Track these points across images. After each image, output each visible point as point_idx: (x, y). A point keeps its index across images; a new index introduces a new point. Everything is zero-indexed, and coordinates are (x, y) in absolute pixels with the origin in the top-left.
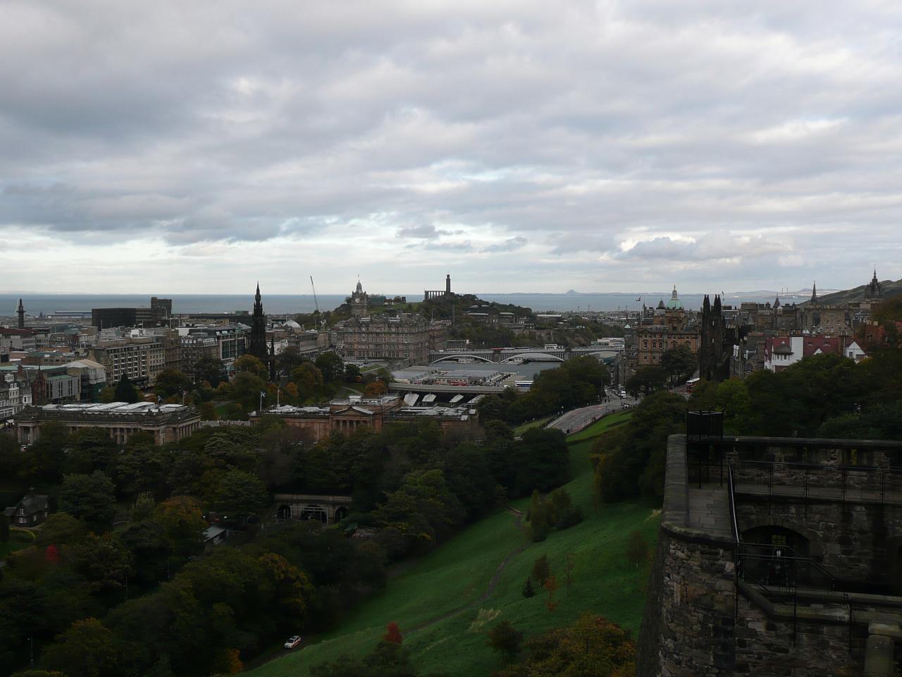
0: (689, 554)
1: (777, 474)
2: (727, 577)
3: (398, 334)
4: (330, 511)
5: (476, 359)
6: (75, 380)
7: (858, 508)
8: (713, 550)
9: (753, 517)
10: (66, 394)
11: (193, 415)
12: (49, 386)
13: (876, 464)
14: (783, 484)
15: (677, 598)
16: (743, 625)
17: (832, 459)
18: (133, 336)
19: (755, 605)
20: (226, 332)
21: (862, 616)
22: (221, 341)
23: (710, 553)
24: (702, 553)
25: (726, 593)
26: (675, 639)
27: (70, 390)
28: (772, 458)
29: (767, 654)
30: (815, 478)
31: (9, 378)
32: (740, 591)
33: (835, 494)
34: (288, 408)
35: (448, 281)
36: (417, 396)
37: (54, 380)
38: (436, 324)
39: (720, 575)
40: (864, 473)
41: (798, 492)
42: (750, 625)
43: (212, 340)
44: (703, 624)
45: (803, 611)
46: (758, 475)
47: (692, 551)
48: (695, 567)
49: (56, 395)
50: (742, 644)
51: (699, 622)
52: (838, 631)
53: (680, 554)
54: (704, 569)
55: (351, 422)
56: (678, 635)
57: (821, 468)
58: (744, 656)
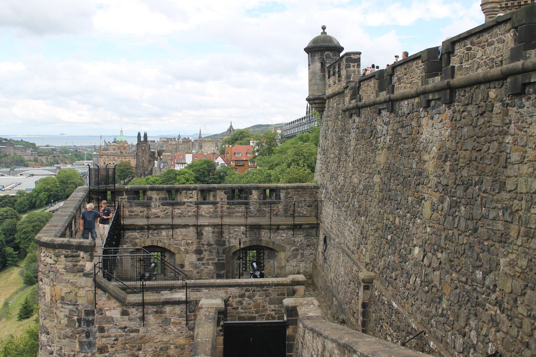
0: (56, 259)
1: (154, 211)
2: (86, 275)
7: (207, 229)
8: (74, 254)
9: (137, 241)
13: (218, 200)
14: (158, 217)
15: (48, 298)
16: (102, 314)
17: (190, 198)
19: (112, 296)
21: (193, 295)
23: (73, 256)
24: (66, 257)
25: (87, 289)
26: (48, 333)
28: (150, 199)
29: (121, 336)
30: (180, 211)
32: (97, 285)
33: (192, 221)
39: (81, 274)
40: (211, 206)
41: (168, 221)
42: (108, 314)
44: (69, 317)
45: (150, 297)
46: (141, 212)
47: (58, 256)
48: (60, 270)
50: (102, 330)
51: (66, 316)
52: (178, 309)
53: (49, 261)
54: (68, 270)
56: (49, 330)
57: (184, 203)
58: (104, 339)
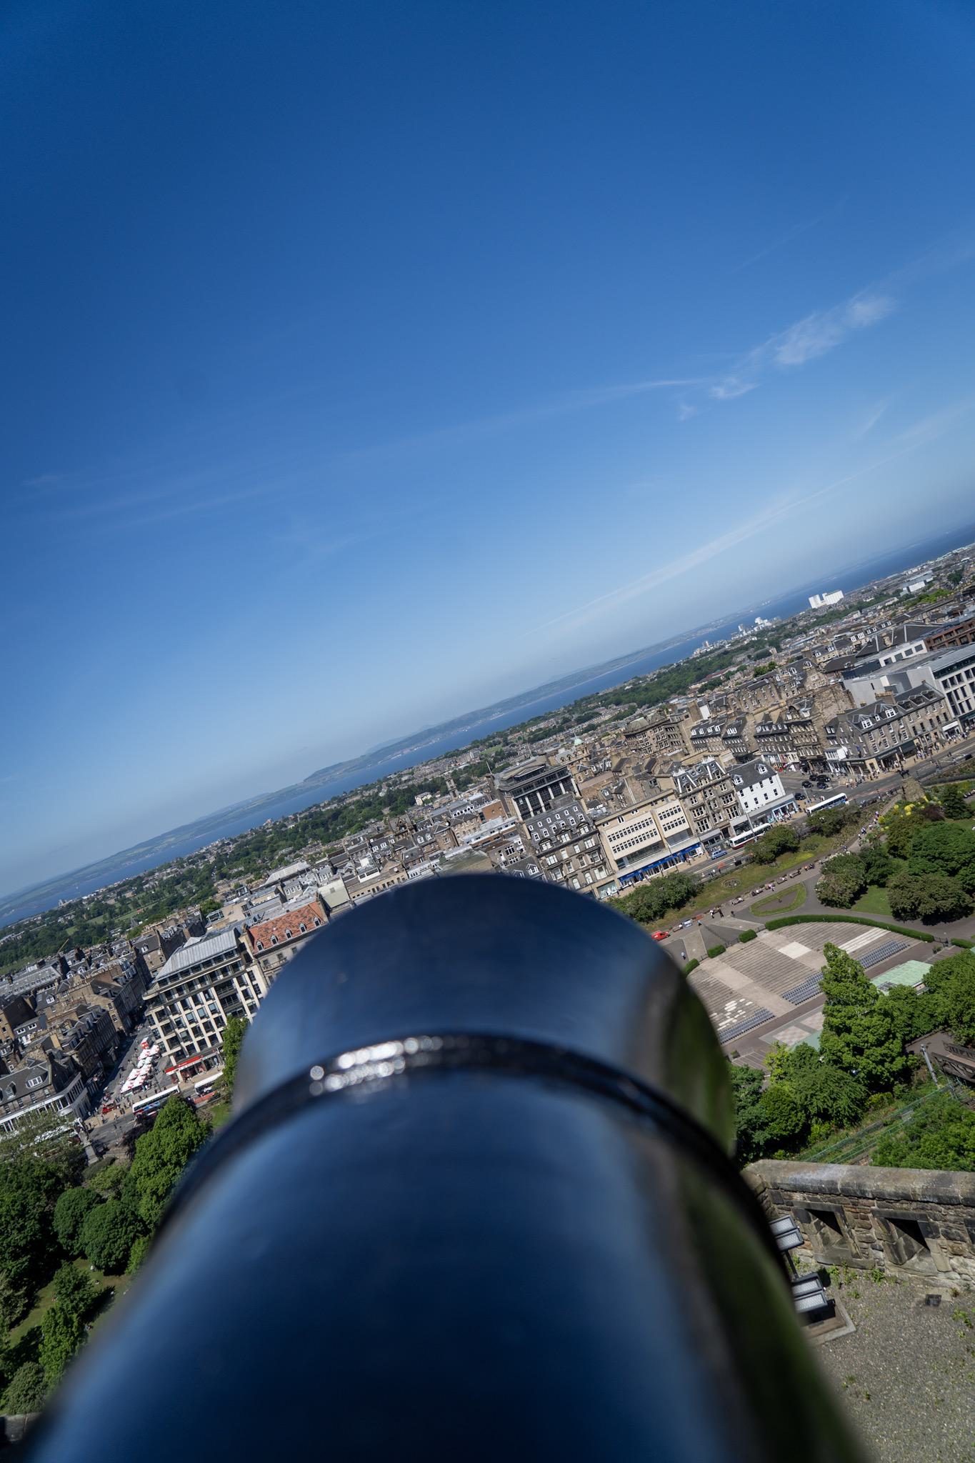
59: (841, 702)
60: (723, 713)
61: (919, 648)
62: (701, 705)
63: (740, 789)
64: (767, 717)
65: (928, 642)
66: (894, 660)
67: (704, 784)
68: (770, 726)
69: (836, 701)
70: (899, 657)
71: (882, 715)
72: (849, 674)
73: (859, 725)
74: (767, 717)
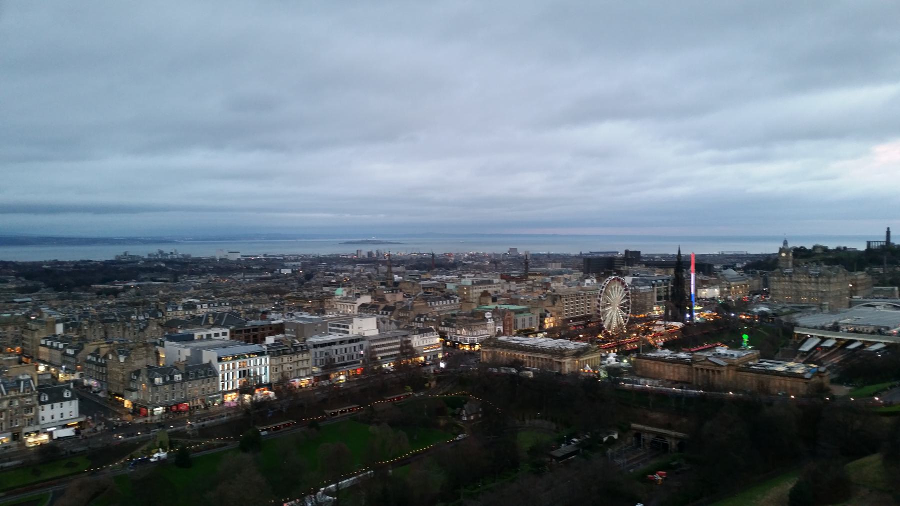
3: (817, 283)
4: (673, 444)
5: (895, 306)
6: (534, 317)
10: (527, 327)
11: (592, 352)
12: (516, 321)
18: (588, 284)
20: (660, 281)
22: (656, 288)
27: (531, 324)
31: (488, 315)
34: (667, 353)
35: (888, 233)
36: (818, 340)
37: (519, 318)
38: (861, 275)
43: (648, 287)
49: (520, 327)
55: (708, 370)
59: (150, 359)
60: (73, 335)
61: (225, 334)
62: (58, 322)
63: (42, 403)
64: (98, 350)
65: (232, 332)
66: (205, 337)
67: (13, 394)
68: (98, 358)
69: (147, 357)
70: (209, 336)
71: (172, 377)
72: (171, 339)
73: (152, 381)
74: (98, 350)
